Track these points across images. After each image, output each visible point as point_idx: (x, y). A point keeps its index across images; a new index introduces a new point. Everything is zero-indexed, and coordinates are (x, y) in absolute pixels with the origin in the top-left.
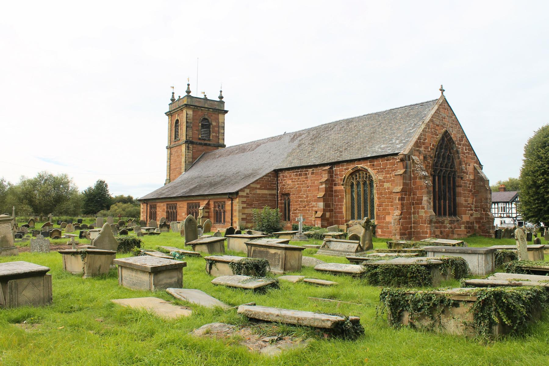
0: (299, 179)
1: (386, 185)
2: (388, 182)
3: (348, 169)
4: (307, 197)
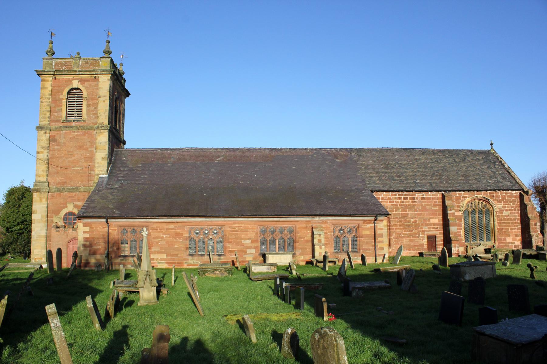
0: (403, 202)
1: (505, 213)
2: (507, 210)
3: (466, 197)
4: (415, 221)
